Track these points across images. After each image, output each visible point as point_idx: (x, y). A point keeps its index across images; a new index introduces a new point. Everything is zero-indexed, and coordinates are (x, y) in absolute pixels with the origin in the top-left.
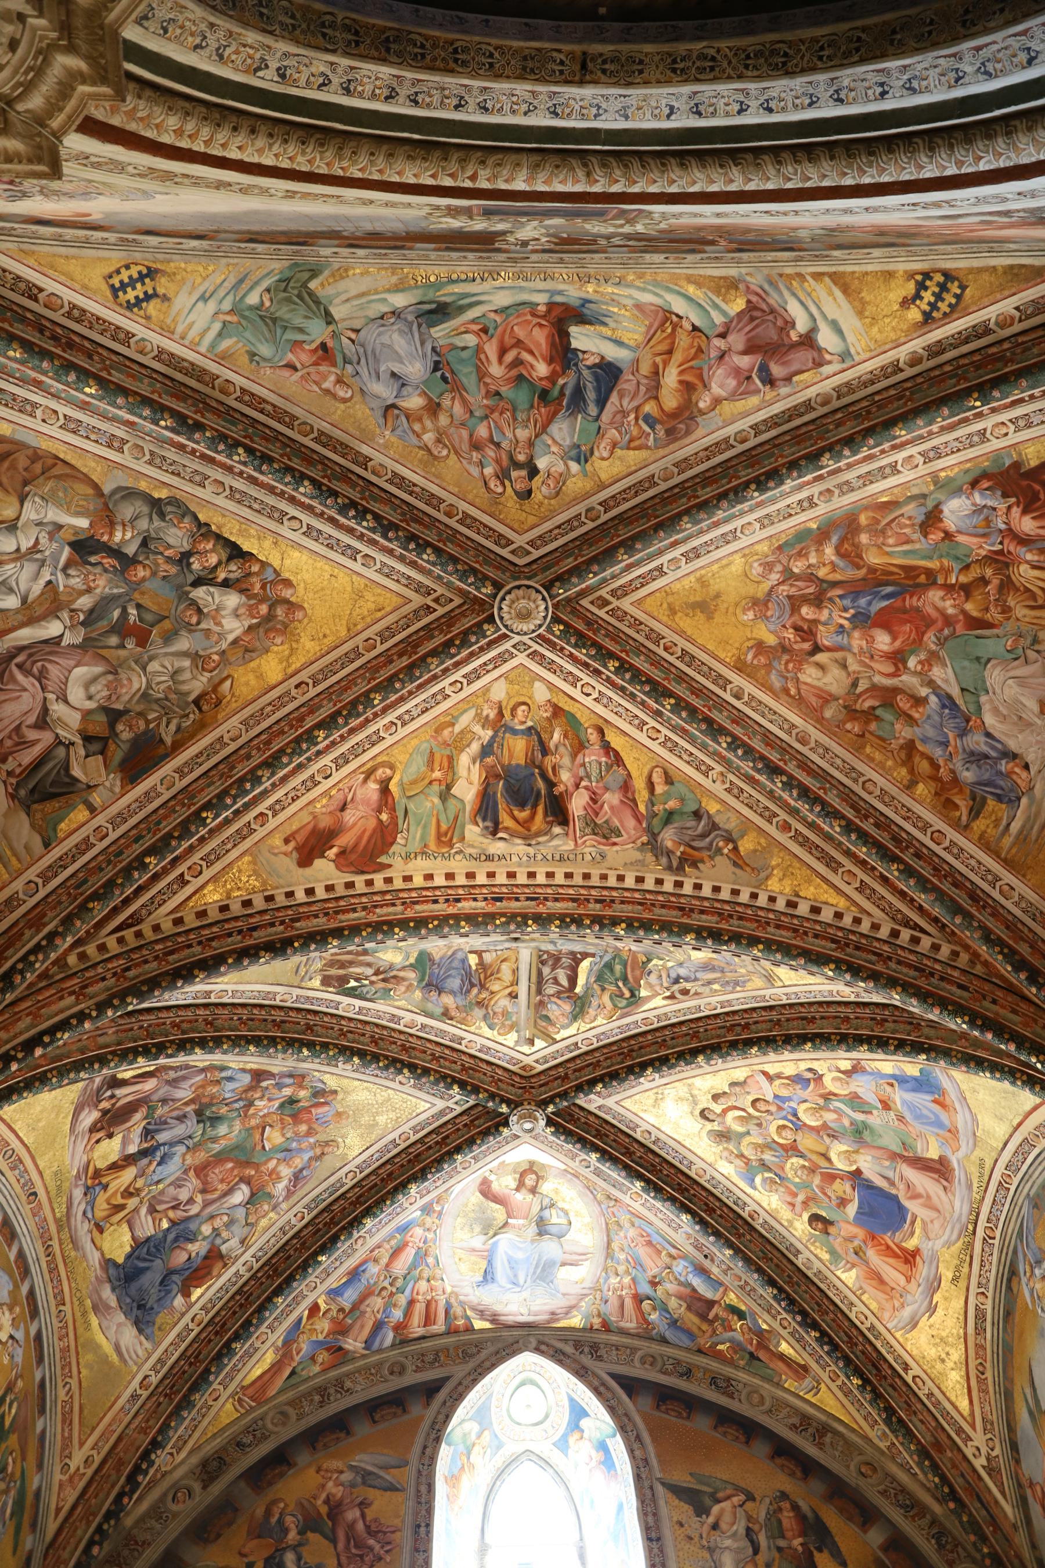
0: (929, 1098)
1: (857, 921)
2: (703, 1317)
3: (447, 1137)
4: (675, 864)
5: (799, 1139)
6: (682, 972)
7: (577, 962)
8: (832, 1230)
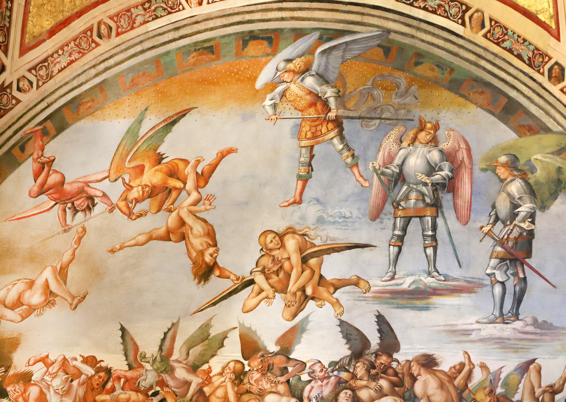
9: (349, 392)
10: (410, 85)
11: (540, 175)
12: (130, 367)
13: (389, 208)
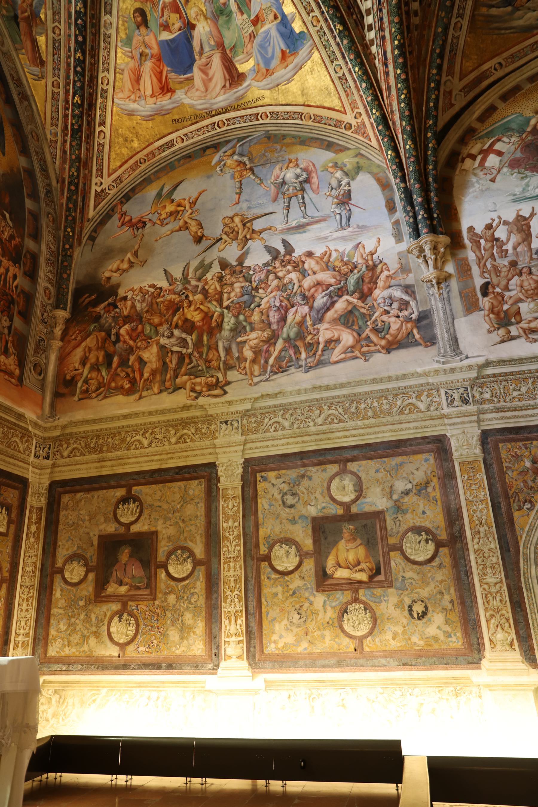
0: (283, 47)
8: (143, 29)
10: (282, 147)
12: (170, 285)
13: (280, 196)
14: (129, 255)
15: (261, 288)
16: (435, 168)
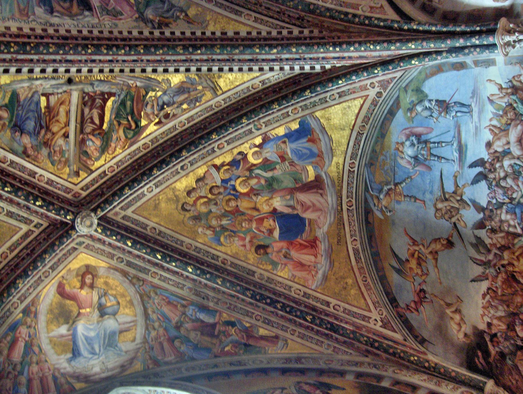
0: (305, 140)
1: (259, 33)
2: (212, 335)
3: (34, 249)
4: (156, 26)
5: (239, 204)
6: (166, 98)
7: (105, 101)
9: (501, 181)
10: (382, 154)
11: (414, 99)
12: (487, 279)
13: (427, 163)
14: (448, 311)
15: (512, 195)
16: (436, 25)
